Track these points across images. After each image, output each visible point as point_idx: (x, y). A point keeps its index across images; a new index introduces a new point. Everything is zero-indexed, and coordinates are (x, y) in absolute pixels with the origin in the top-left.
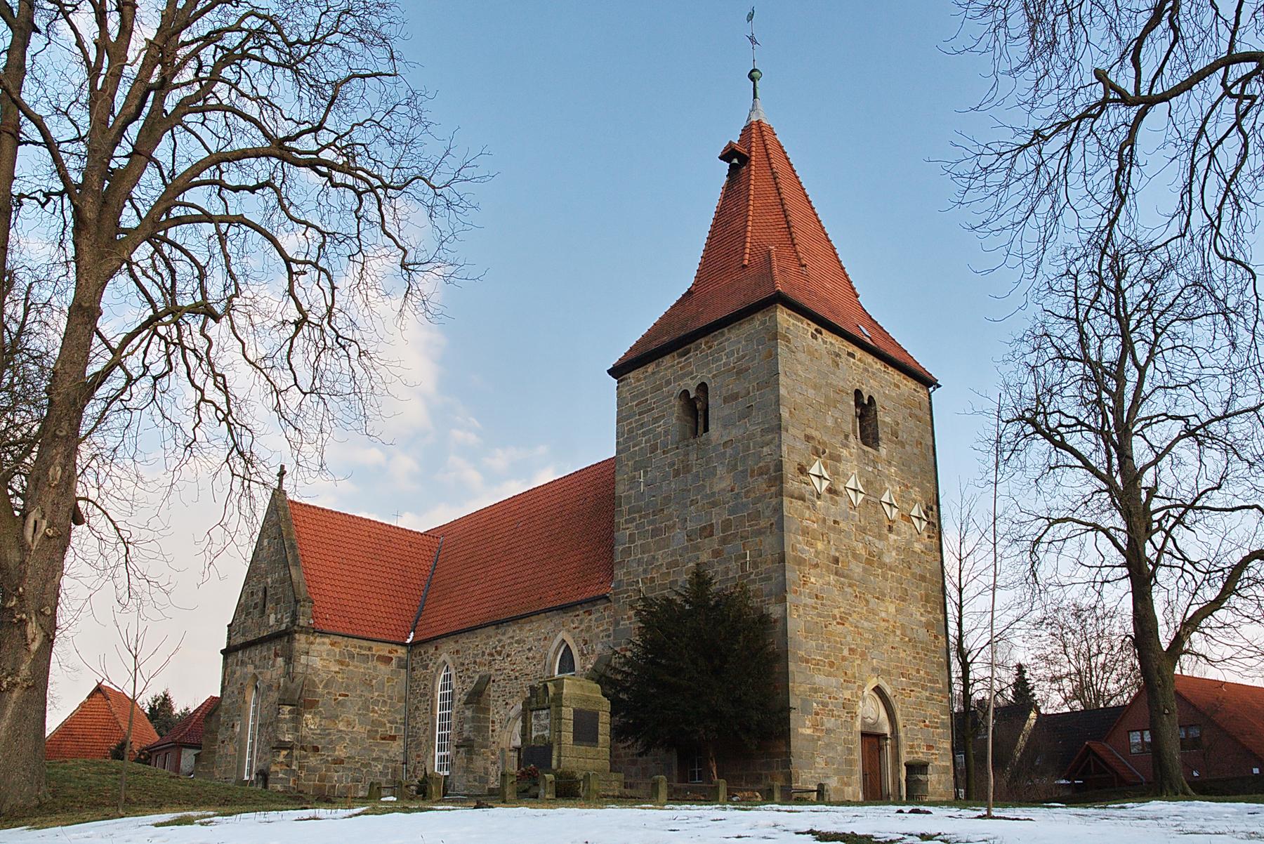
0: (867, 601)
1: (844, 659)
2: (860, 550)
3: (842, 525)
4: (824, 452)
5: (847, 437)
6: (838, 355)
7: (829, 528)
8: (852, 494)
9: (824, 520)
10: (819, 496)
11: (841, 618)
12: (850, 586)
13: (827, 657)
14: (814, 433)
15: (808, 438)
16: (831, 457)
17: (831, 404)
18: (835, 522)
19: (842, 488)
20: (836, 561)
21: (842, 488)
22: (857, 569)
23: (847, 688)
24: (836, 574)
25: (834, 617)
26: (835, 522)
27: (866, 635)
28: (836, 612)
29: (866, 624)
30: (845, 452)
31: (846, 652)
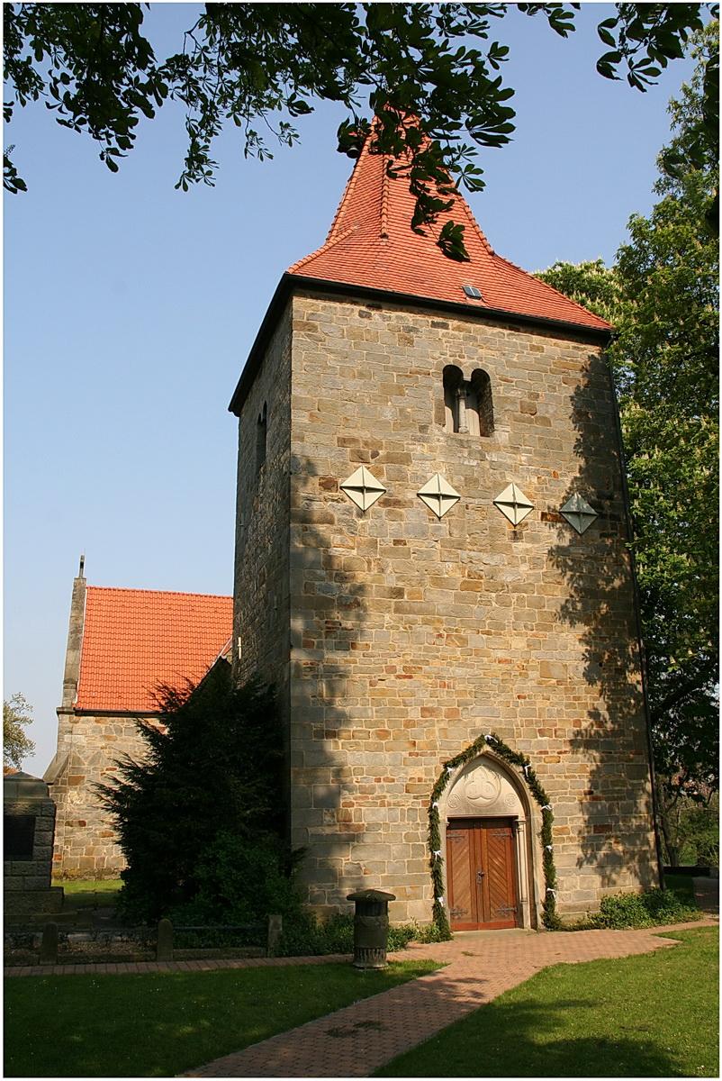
0: (464, 641)
1: (409, 724)
2: (450, 570)
3: (413, 545)
4: (375, 455)
5: (423, 428)
6: (410, 330)
7: (384, 552)
8: (432, 503)
9: (373, 544)
10: (362, 513)
11: (405, 669)
12: (426, 622)
13: (375, 724)
14: (355, 434)
15: (343, 442)
16: (390, 459)
17: (388, 391)
18: (397, 542)
19: (411, 495)
20: (398, 593)
21: (411, 495)
22: (443, 600)
23: (416, 764)
24: (397, 610)
25: (392, 669)
26: (397, 542)
27: (460, 687)
28: (394, 662)
29: (460, 671)
30: (418, 449)
31: (414, 714)
